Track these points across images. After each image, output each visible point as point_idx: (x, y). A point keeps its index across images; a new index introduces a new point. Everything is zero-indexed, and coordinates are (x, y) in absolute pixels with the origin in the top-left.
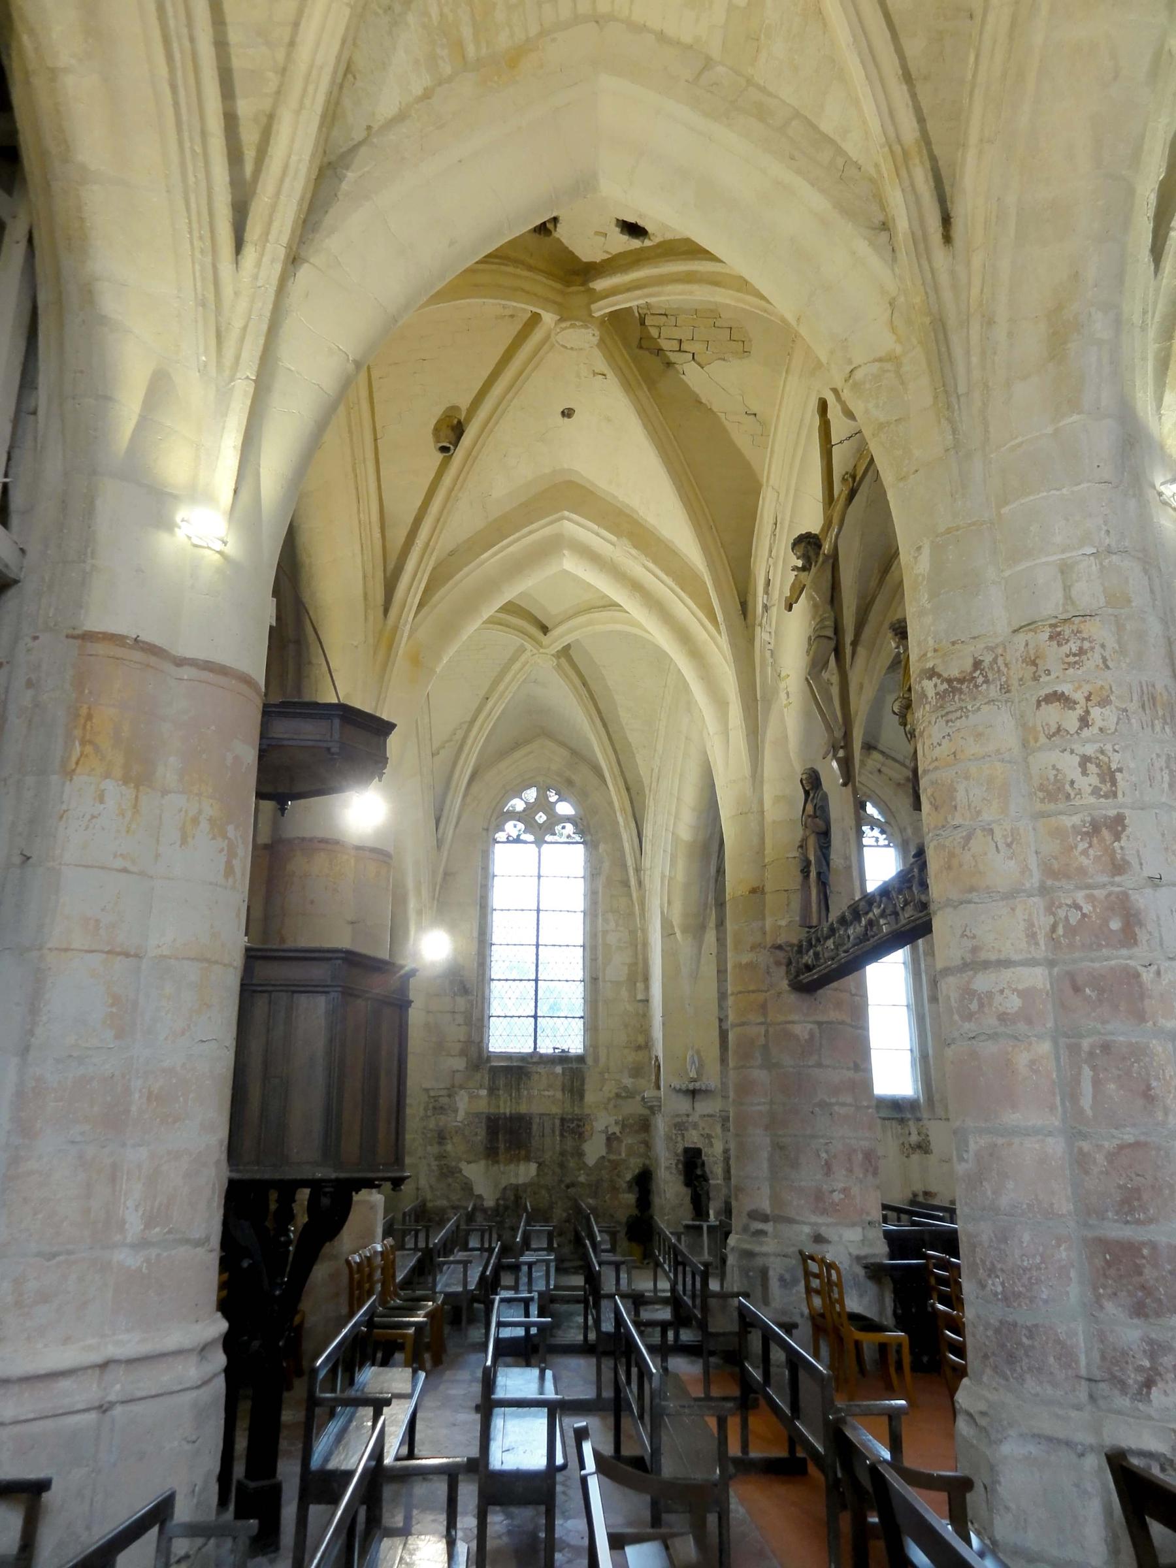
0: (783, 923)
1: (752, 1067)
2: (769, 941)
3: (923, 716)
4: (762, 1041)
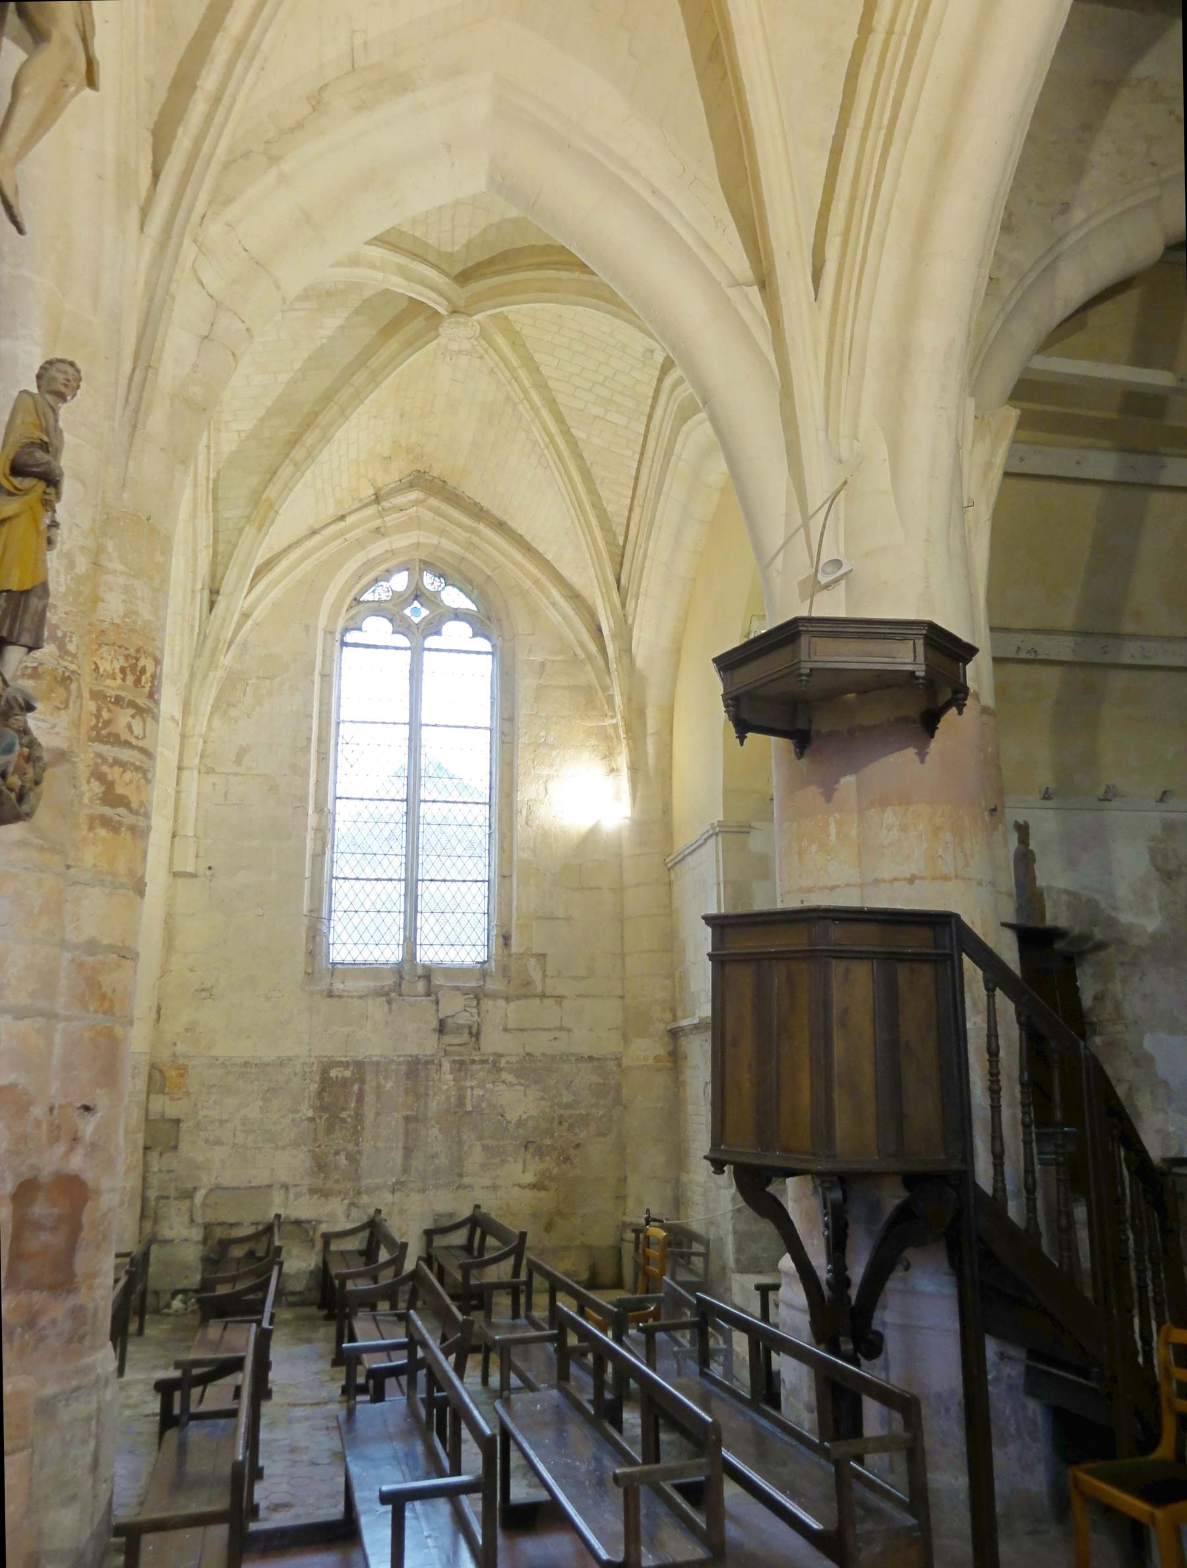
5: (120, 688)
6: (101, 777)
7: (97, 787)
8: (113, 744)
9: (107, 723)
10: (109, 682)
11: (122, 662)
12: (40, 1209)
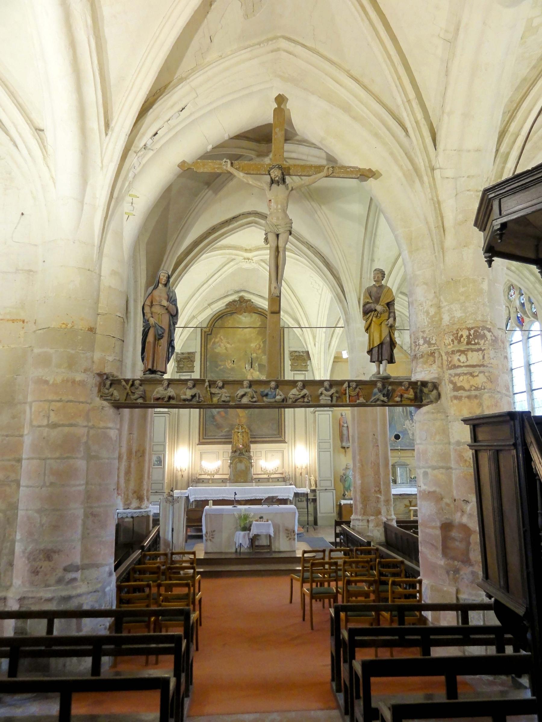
0: (110, 359)
1: (77, 458)
2: (96, 369)
3: (484, 344)
4: (84, 439)
5: (453, 347)
6: (451, 382)
7: (451, 386)
8: (453, 369)
9: (450, 362)
10: (449, 347)
11: (452, 337)
12: (454, 533)
